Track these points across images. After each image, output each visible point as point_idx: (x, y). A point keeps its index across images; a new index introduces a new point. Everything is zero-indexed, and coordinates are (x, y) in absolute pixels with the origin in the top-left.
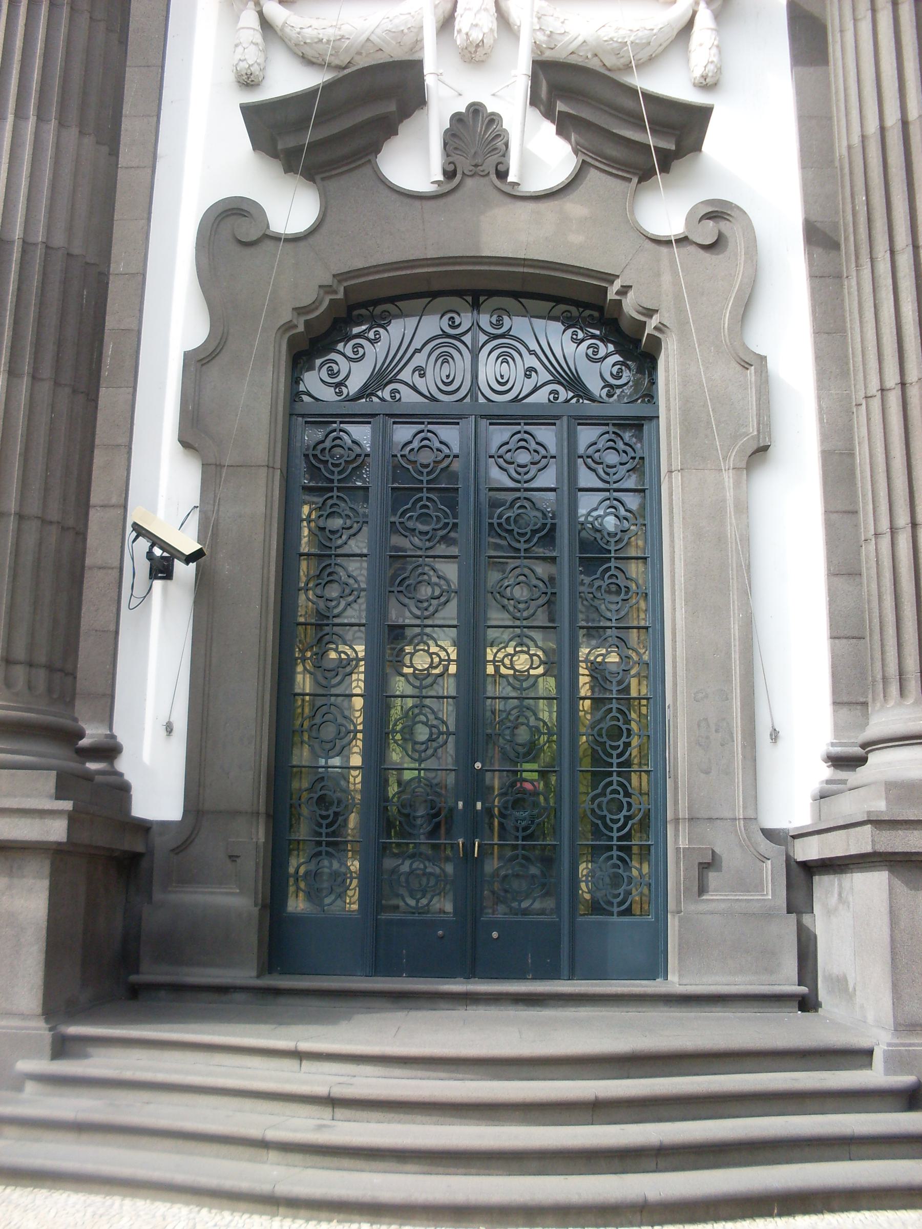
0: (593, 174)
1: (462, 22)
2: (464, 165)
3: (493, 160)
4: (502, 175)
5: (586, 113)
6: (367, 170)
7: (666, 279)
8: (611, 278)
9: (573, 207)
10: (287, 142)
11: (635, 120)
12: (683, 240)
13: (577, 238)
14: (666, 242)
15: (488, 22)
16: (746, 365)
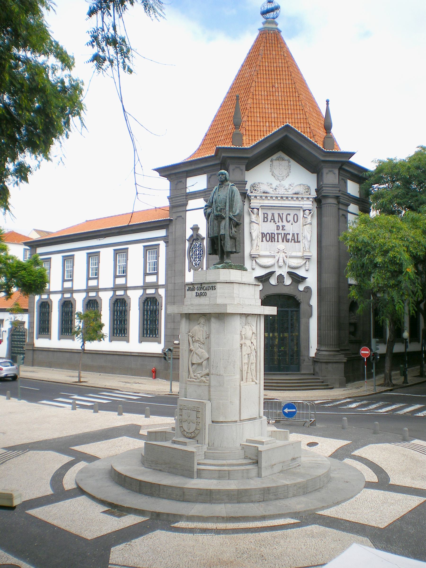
0: (294, 283)
1: (280, 264)
2: (279, 282)
3: (282, 281)
4: (284, 282)
5: (293, 277)
6: (268, 282)
7: (302, 296)
8: (296, 296)
9: (292, 287)
10: (260, 280)
11: (299, 278)
12: (303, 291)
13: (292, 291)
14: (301, 291)
15: (282, 264)
16: (310, 306)
